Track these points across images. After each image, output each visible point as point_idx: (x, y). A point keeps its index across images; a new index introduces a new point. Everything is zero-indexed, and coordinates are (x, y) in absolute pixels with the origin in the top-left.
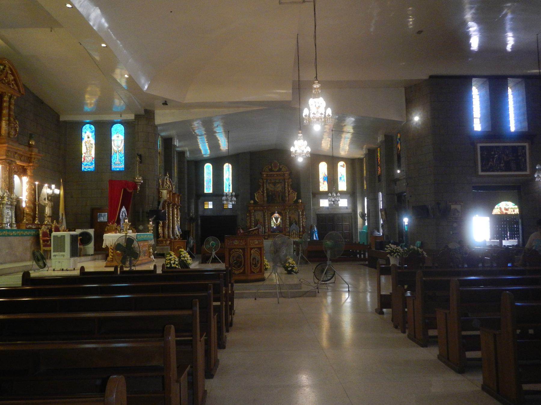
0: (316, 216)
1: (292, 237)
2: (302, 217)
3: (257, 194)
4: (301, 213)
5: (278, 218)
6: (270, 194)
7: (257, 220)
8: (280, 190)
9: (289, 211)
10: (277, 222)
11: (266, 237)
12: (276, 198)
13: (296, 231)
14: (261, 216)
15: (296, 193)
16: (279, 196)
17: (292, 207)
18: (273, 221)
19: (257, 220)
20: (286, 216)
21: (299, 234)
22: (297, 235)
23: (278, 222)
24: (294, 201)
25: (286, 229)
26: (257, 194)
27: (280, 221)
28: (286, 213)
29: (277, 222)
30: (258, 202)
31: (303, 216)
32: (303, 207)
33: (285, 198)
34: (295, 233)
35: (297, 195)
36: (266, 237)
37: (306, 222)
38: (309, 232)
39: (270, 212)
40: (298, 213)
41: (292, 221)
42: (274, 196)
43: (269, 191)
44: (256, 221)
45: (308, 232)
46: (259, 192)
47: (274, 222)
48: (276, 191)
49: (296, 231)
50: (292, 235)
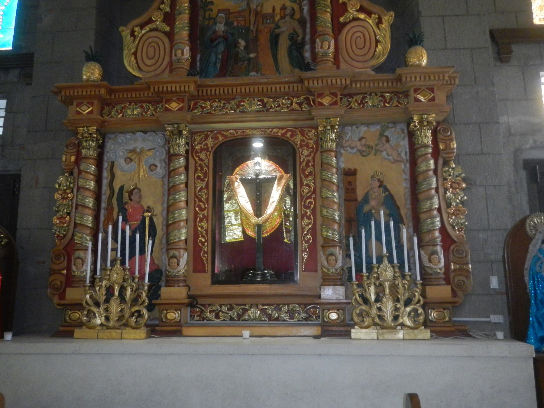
0: (523, 174)
1: (367, 321)
2: (435, 171)
3: (132, 34)
4: (427, 137)
5: (270, 182)
6: (221, 28)
7: (122, 188)
8: (284, 8)
9: (343, 125)
10: (259, 208)
11: (173, 315)
12: (252, 55)
13: (403, 277)
14: (152, 167)
15: (388, 18)
16: (275, 40)
17: (362, 103)
18: (235, 206)
19: (126, 195)
20: (325, 165)
21: (423, 294)
22: (407, 303)
23: (270, 209)
24: (374, 62)
25: (322, 257)
26: (132, 34)
27: (282, 199)
28: (320, 140)
29: (259, 208)
30: (140, 78)
31: (446, 163)
32: (441, 96)
33: (313, 49)
34: (394, 287)
35: (393, 27)
36: (173, 315)
37: (462, 202)
38: (494, 283)
39: (210, 142)
40: (405, 143)
41: (366, 199)
42: (242, 43)
43: (213, 14)
44: (114, 201)
45: (487, 282)
46: (150, 21)
47: (240, 211)
48: (253, 6)
49: (403, 277)
50: (366, 301)
